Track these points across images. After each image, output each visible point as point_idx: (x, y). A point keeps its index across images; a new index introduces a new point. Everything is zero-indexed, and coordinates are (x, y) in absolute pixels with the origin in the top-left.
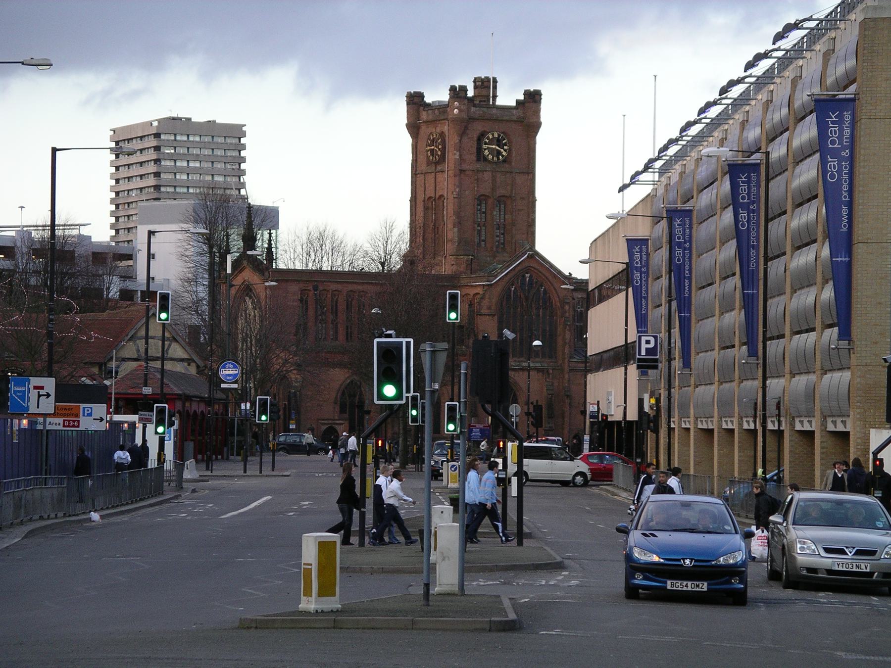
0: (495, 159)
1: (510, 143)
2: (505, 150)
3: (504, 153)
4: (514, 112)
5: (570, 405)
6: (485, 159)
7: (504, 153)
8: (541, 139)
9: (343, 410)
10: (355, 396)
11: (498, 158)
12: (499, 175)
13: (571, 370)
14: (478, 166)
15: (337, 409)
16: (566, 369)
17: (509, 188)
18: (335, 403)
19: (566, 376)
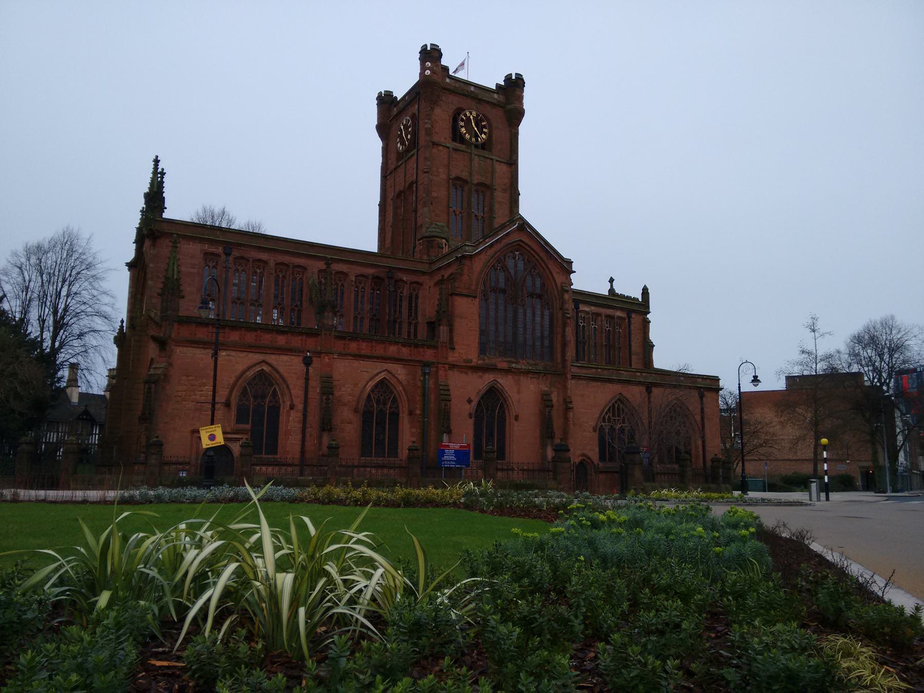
0: (474, 139)
1: (490, 126)
3: (483, 136)
6: (462, 140)
8: (523, 128)
10: (264, 397)
11: (477, 140)
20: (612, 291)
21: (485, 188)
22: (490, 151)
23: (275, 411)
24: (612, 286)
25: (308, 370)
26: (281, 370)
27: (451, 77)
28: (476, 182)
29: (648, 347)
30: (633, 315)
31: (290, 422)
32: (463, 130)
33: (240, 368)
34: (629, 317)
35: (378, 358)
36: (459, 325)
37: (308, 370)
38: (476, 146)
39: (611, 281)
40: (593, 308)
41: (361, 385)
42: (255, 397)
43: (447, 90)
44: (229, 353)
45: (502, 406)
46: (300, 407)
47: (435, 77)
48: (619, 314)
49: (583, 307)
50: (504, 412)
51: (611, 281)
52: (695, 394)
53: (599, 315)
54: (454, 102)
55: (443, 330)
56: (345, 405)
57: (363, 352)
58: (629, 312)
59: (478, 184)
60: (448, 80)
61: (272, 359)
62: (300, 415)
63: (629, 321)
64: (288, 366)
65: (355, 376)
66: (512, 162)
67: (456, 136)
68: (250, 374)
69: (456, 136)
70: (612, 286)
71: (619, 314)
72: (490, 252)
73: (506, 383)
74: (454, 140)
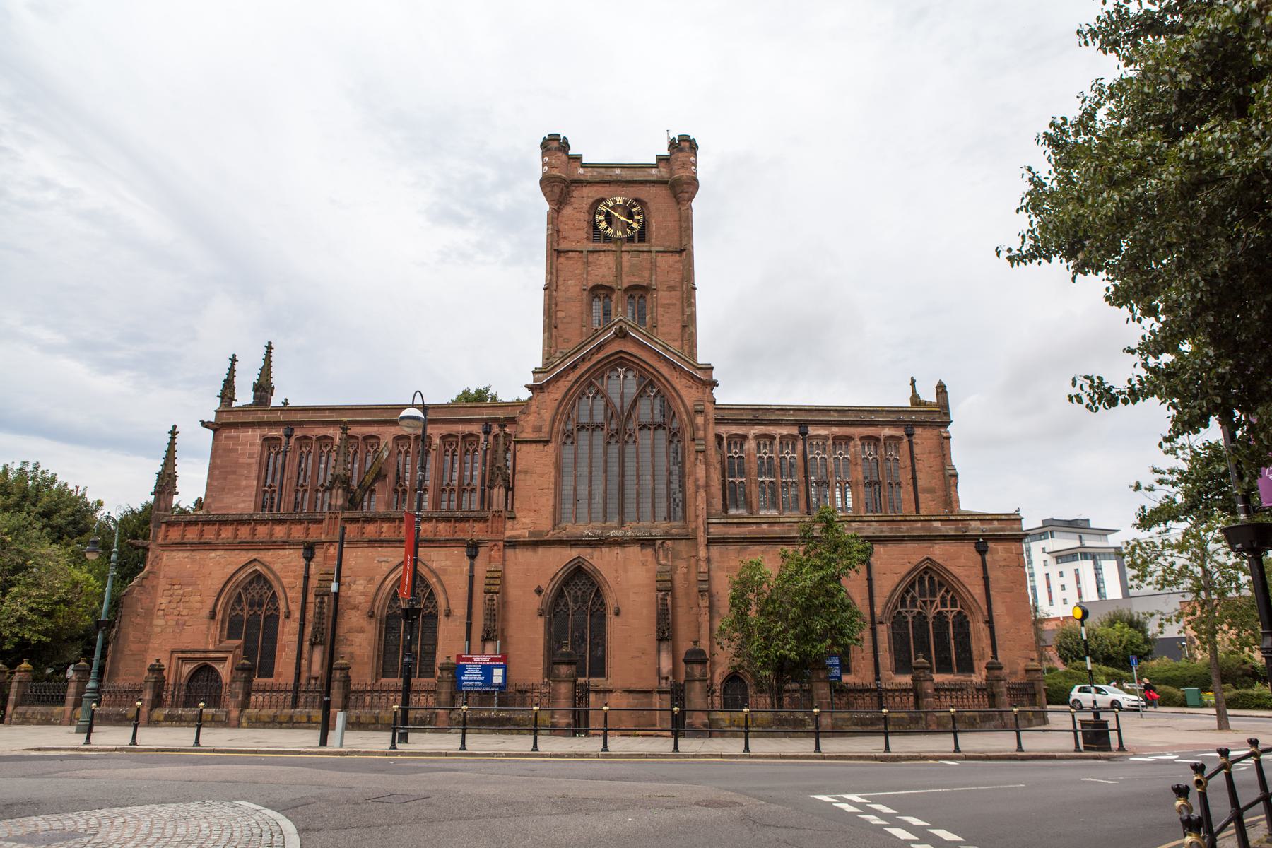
0: (619, 233)
2: (638, 221)
4: (654, 171)
5: (711, 608)
6: (608, 239)
7: (635, 225)
9: (233, 633)
10: (260, 605)
12: (626, 257)
13: (711, 542)
14: (591, 246)
15: (215, 628)
16: (702, 540)
17: (646, 274)
18: (213, 616)
19: (702, 553)
20: (915, 398)
21: (638, 292)
22: (649, 241)
23: (272, 620)
24: (914, 391)
25: (308, 567)
26: (276, 567)
27: (584, 166)
28: (625, 285)
29: (949, 478)
30: (918, 431)
31: (288, 634)
32: (603, 225)
33: (231, 570)
34: (910, 435)
35: (388, 542)
36: (523, 484)
37: (308, 567)
38: (630, 240)
39: (913, 382)
40: (836, 430)
41: (378, 580)
42: (251, 605)
43: (580, 183)
44: (218, 553)
45: (598, 594)
46: (297, 614)
47: (555, 172)
48: (887, 431)
49: (812, 431)
50: (603, 604)
51: (913, 382)
52: (969, 549)
53: (849, 439)
54: (591, 193)
55: (498, 494)
56: (356, 608)
57: (384, 536)
58: (909, 427)
59: (626, 290)
60: (580, 171)
61: (267, 556)
62: (296, 625)
63: (910, 442)
64: (285, 566)
65: (370, 570)
66: (683, 251)
67: (596, 234)
68: (242, 575)
69: (596, 234)
70: (914, 391)
71: (887, 431)
72: (573, 377)
73: (602, 561)
74: (596, 240)
